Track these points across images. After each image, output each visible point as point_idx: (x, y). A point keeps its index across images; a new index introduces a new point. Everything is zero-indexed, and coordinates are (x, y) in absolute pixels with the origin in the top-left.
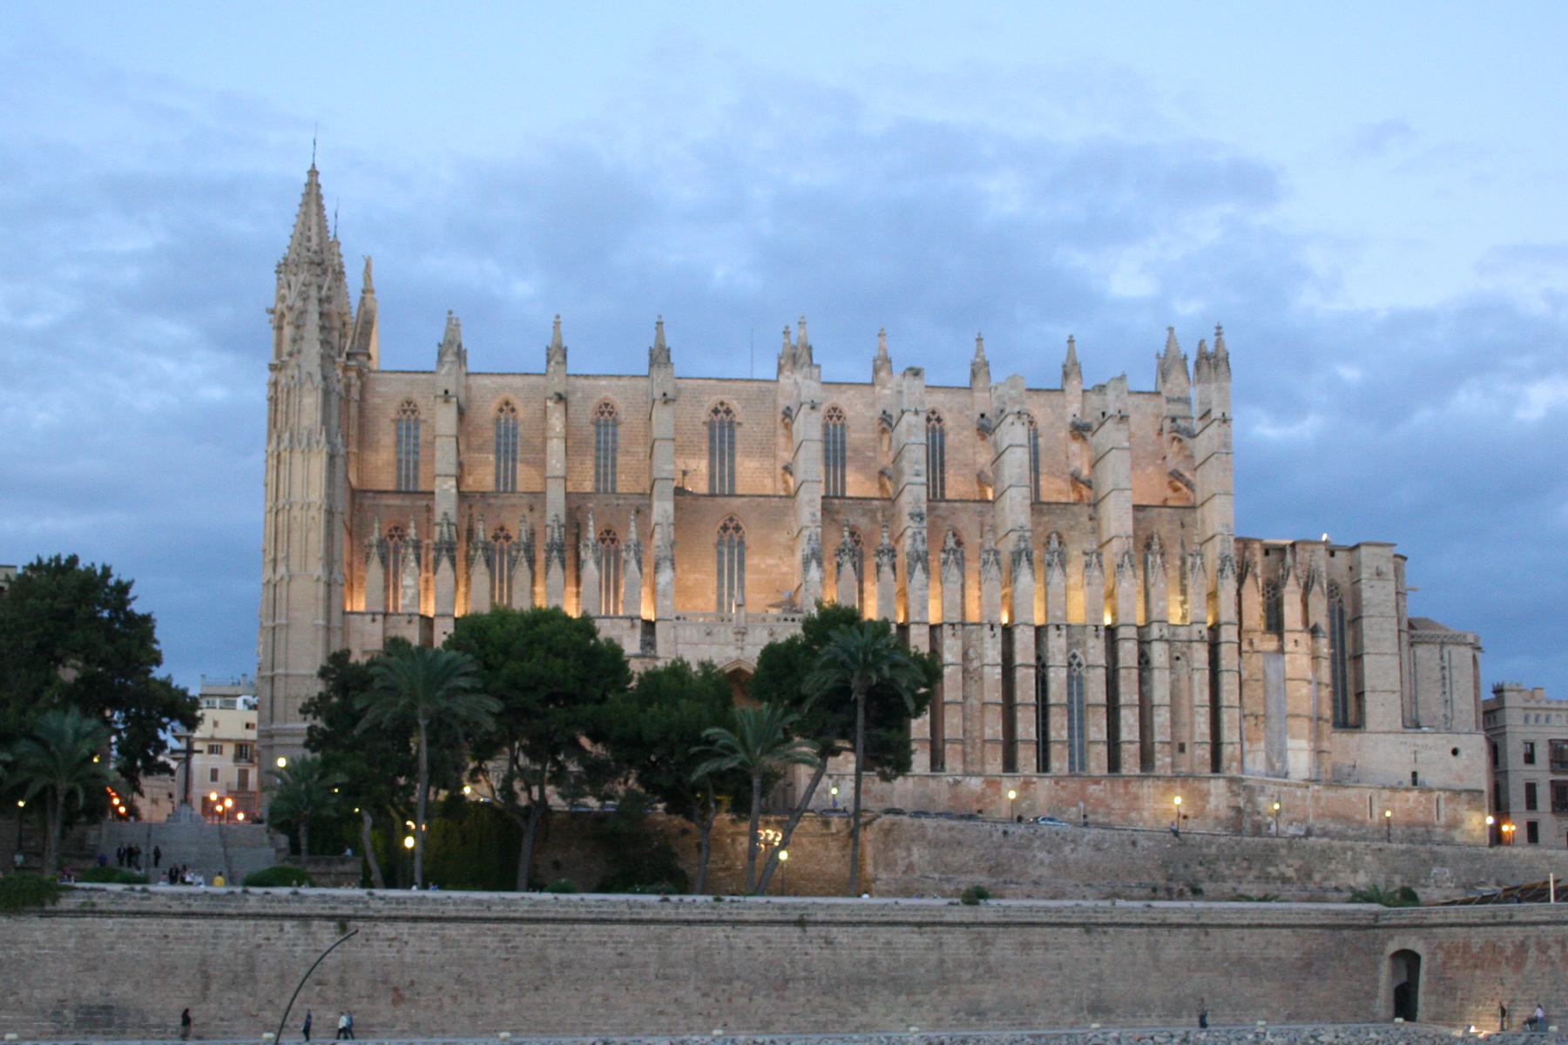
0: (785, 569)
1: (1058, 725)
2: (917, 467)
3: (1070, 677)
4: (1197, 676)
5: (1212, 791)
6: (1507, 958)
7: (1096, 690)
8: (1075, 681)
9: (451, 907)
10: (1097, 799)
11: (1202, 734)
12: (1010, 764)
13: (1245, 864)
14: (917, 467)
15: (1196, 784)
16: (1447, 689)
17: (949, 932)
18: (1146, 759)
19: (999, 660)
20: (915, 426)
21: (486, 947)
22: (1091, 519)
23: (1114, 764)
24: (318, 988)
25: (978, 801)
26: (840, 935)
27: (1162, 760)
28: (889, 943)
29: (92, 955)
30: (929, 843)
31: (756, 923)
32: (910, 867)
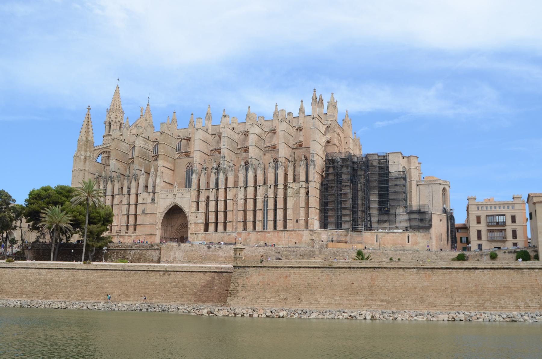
1: (258, 216)
2: (224, 143)
5: (304, 234)
7: (271, 205)
8: (265, 203)
10: (269, 238)
11: (302, 216)
12: (245, 229)
13: (301, 257)
14: (224, 143)
15: (299, 232)
18: (285, 227)
23: (275, 227)
26: (43, 272)
27: (290, 225)
30: (182, 251)
31: (19, 268)
32: (175, 258)
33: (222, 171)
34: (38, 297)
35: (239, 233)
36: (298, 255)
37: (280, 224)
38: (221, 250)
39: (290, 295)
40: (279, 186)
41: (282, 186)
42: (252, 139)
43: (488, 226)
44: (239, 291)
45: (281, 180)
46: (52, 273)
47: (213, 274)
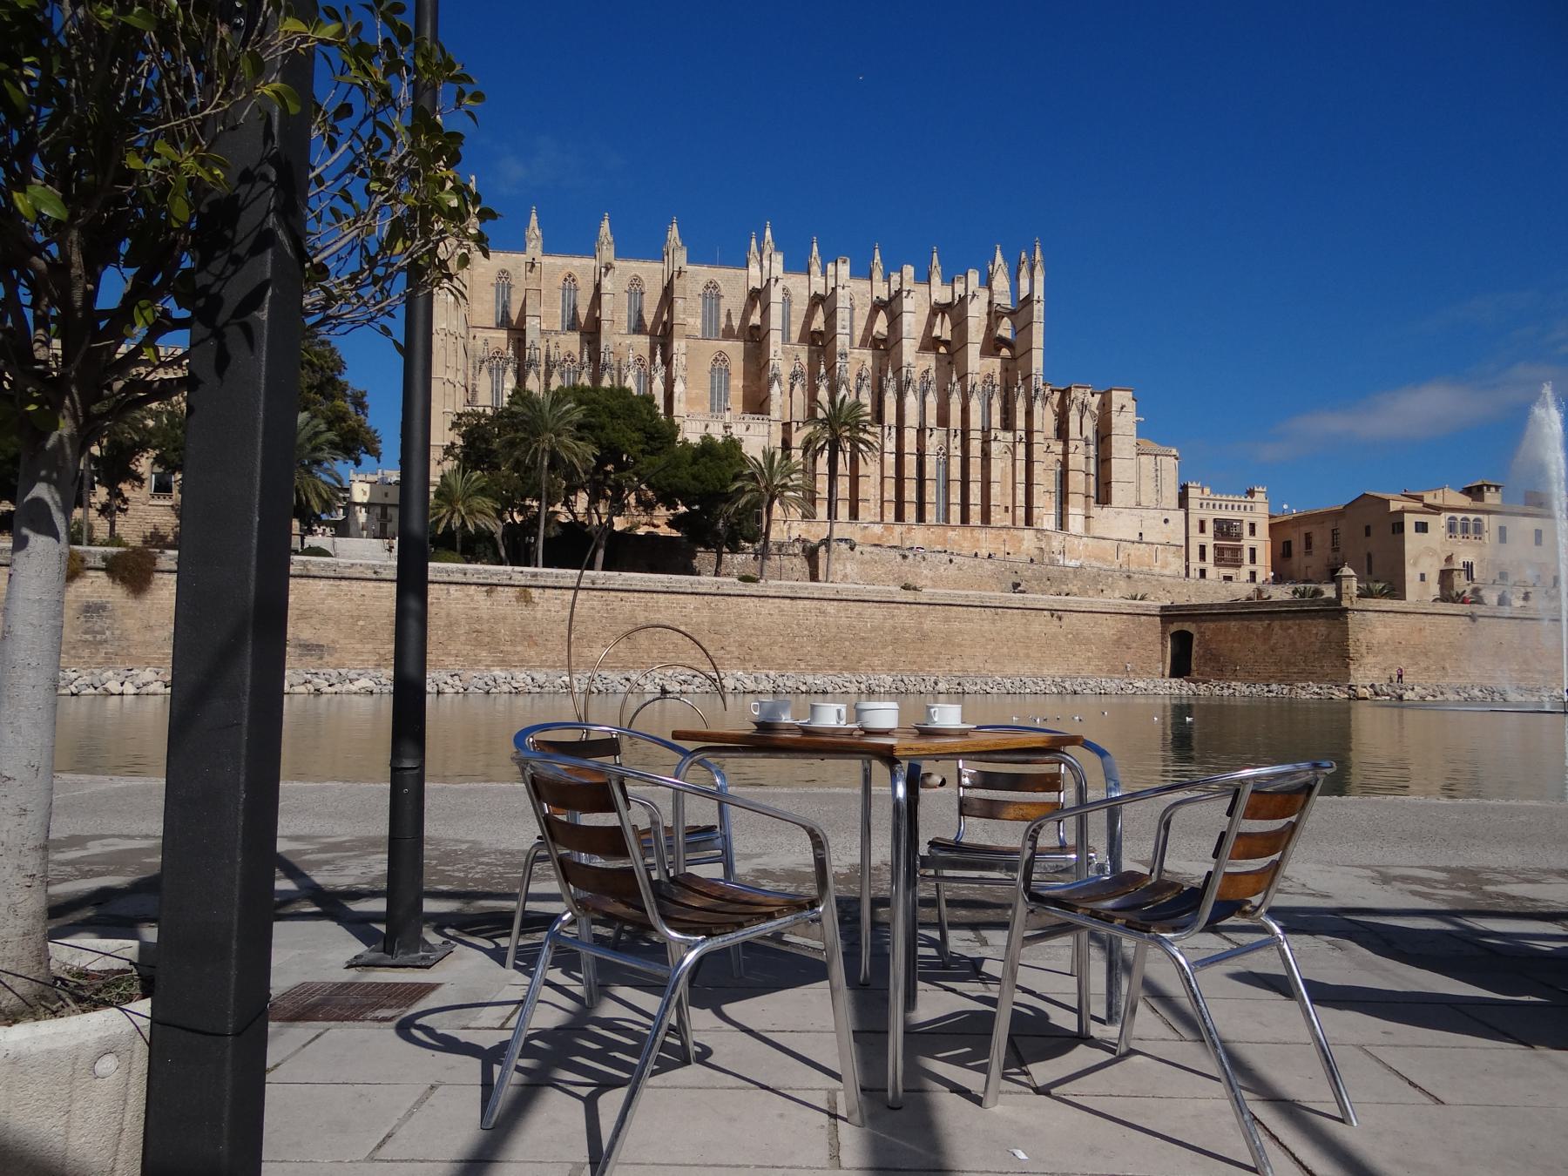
0: (754, 389)
3: (938, 463)
4: (1018, 463)
6: (1257, 636)
7: (955, 472)
9: (569, 580)
12: (900, 517)
15: (1016, 532)
16: (1159, 484)
17: (899, 608)
19: (894, 450)
20: (843, 296)
21: (593, 609)
22: (949, 363)
23: (965, 519)
24: (475, 634)
25: (879, 539)
26: (830, 608)
27: (997, 516)
28: (860, 614)
29: (307, 607)
31: (775, 597)
32: (845, 576)
33: (844, 386)
34: (832, 668)
35: (888, 527)
36: (1045, 580)
37: (975, 512)
38: (924, 563)
39: (1431, 662)
40: (973, 434)
41: (978, 435)
42: (909, 325)
43: (1216, 538)
44: (1365, 654)
45: (976, 420)
46: (847, 610)
47: (1125, 617)
